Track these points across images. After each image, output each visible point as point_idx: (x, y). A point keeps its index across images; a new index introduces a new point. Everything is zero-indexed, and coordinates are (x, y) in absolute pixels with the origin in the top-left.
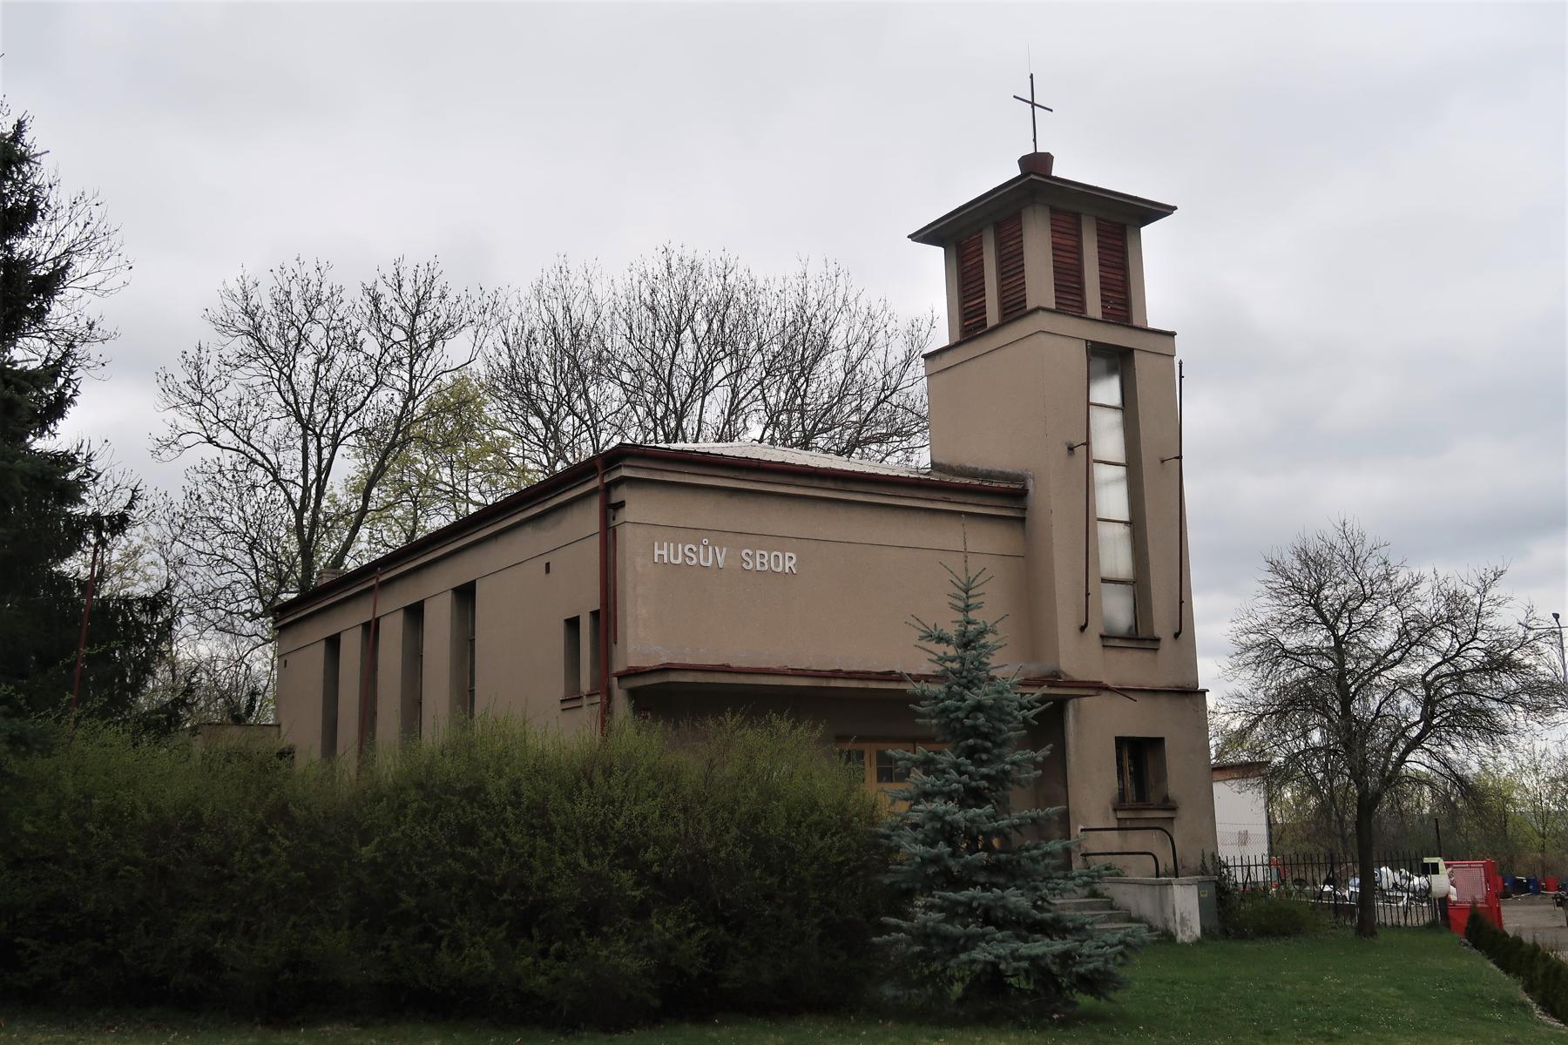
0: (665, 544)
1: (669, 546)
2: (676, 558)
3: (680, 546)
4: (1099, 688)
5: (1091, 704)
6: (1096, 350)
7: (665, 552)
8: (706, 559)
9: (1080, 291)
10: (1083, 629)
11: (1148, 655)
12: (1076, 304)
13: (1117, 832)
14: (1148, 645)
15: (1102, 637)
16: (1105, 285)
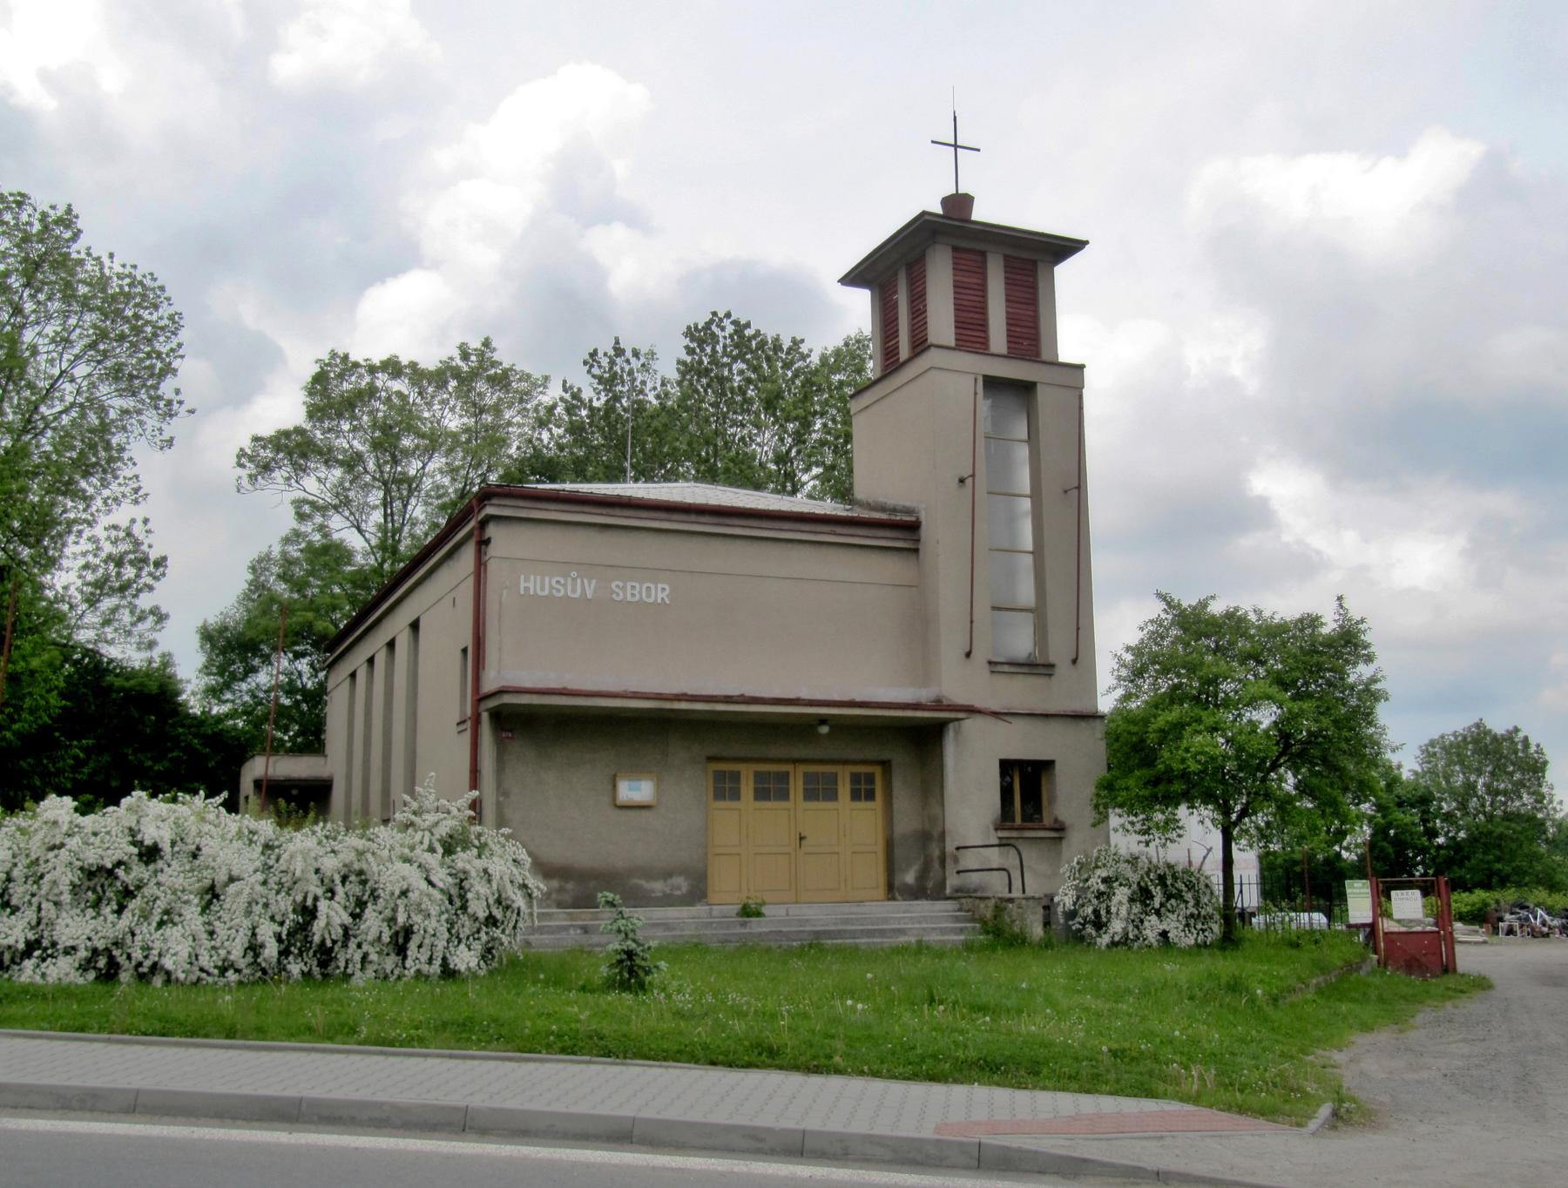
0: (532, 577)
2: (542, 589)
3: (547, 579)
4: (971, 710)
5: (971, 725)
6: (993, 384)
7: (534, 584)
8: (574, 591)
9: (983, 326)
10: (968, 655)
11: (1041, 681)
12: (980, 340)
13: (997, 848)
14: (1042, 670)
15: (990, 663)
16: (1012, 322)
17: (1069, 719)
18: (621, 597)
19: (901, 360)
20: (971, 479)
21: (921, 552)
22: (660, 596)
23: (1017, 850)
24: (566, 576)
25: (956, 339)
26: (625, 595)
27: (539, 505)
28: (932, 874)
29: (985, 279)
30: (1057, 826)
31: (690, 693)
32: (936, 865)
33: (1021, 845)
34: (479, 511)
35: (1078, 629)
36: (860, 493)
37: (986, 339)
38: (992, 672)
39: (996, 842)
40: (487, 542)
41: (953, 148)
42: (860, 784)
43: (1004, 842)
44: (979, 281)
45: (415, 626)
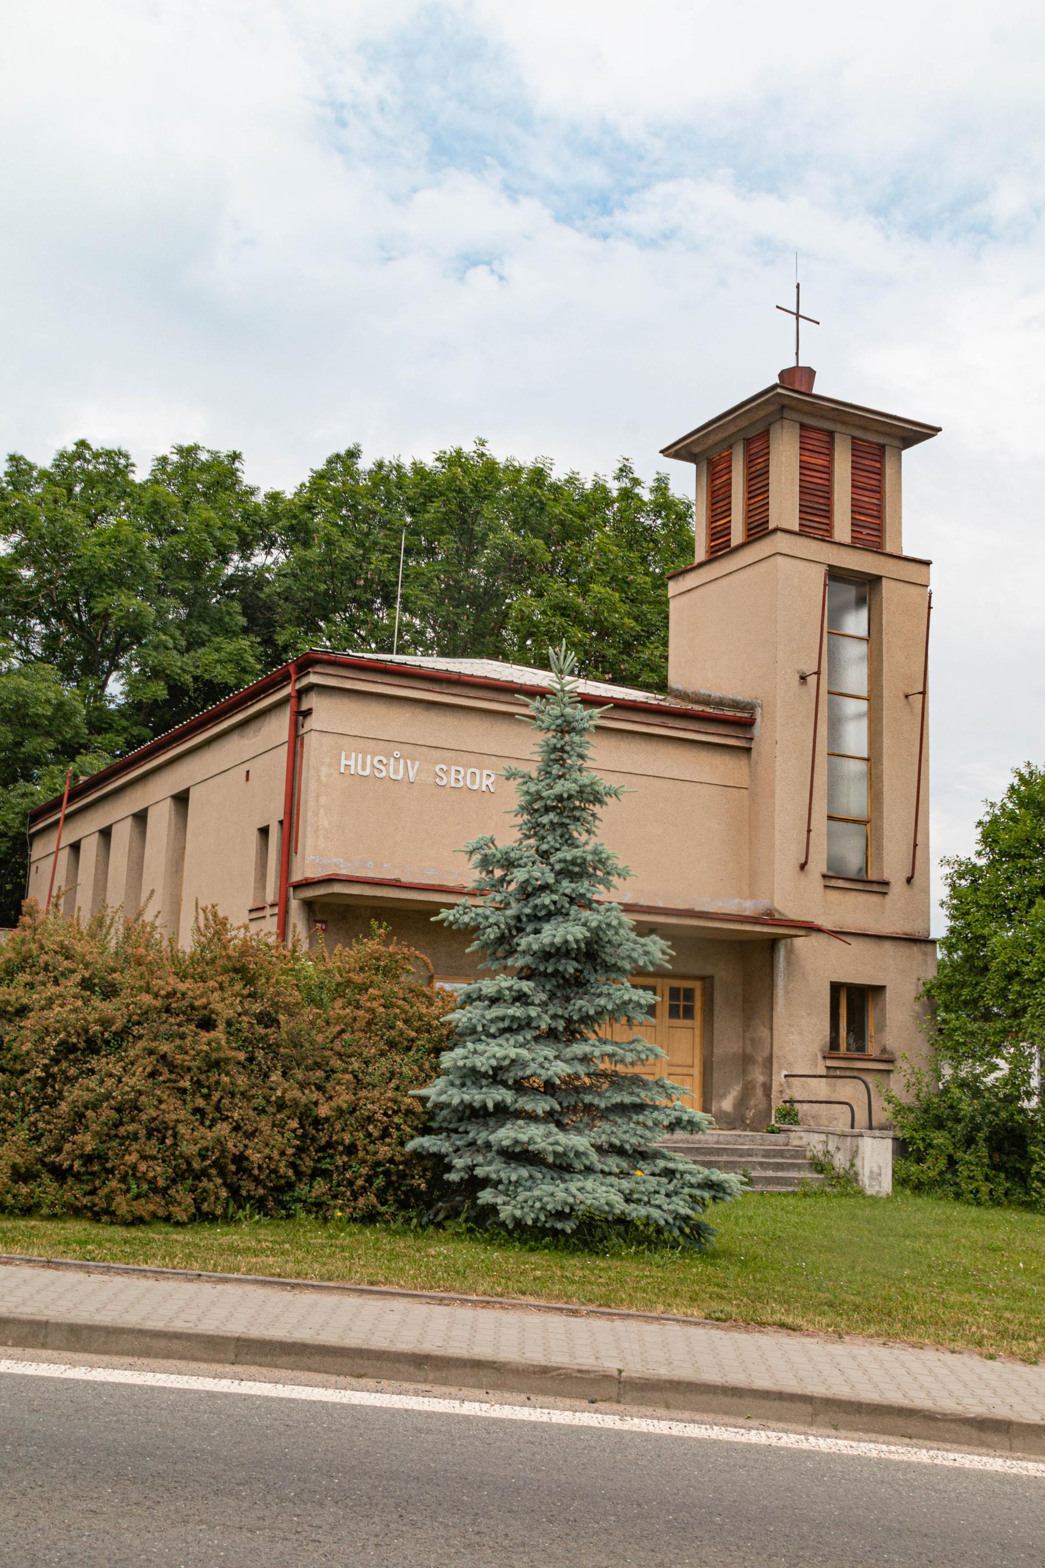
0: (353, 754)
1: (357, 756)
2: (364, 769)
3: (369, 757)
4: (811, 928)
5: (803, 944)
6: (835, 575)
7: (354, 762)
8: (396, 772)
9: (827, 513)
10: (803, 867)
11: (875, 898)
12: (824, 527)
13: (824, 1079)
14: (875, 888)
15: (824, 876)
16: (857, 508)
17: (902, 943)
18: (384, 774)
19: (733, 545)
20: (815, 676)
21: (754, 753)
22: (485, 782)
23: (864, 1082)
24: (389, 755)
25: (800, 525)
26: (388, 772)
27: (363, 676)
28: (752, 1103)
29: (831, 461)
30: (885, 1057)
31: (697, 909)
32: (759, 1092)
33: (869, 1078)
34: (298, 679)
35: (915, 845)
36: (675, 680)
37: (830, 525)
38: (826, 887)
39: (824, 1072)
40: (308, 713)
41: (794, 317)
42: (679, 1000)
43: (832, 1073)
44: (825, 463)
45: (182, 799)
